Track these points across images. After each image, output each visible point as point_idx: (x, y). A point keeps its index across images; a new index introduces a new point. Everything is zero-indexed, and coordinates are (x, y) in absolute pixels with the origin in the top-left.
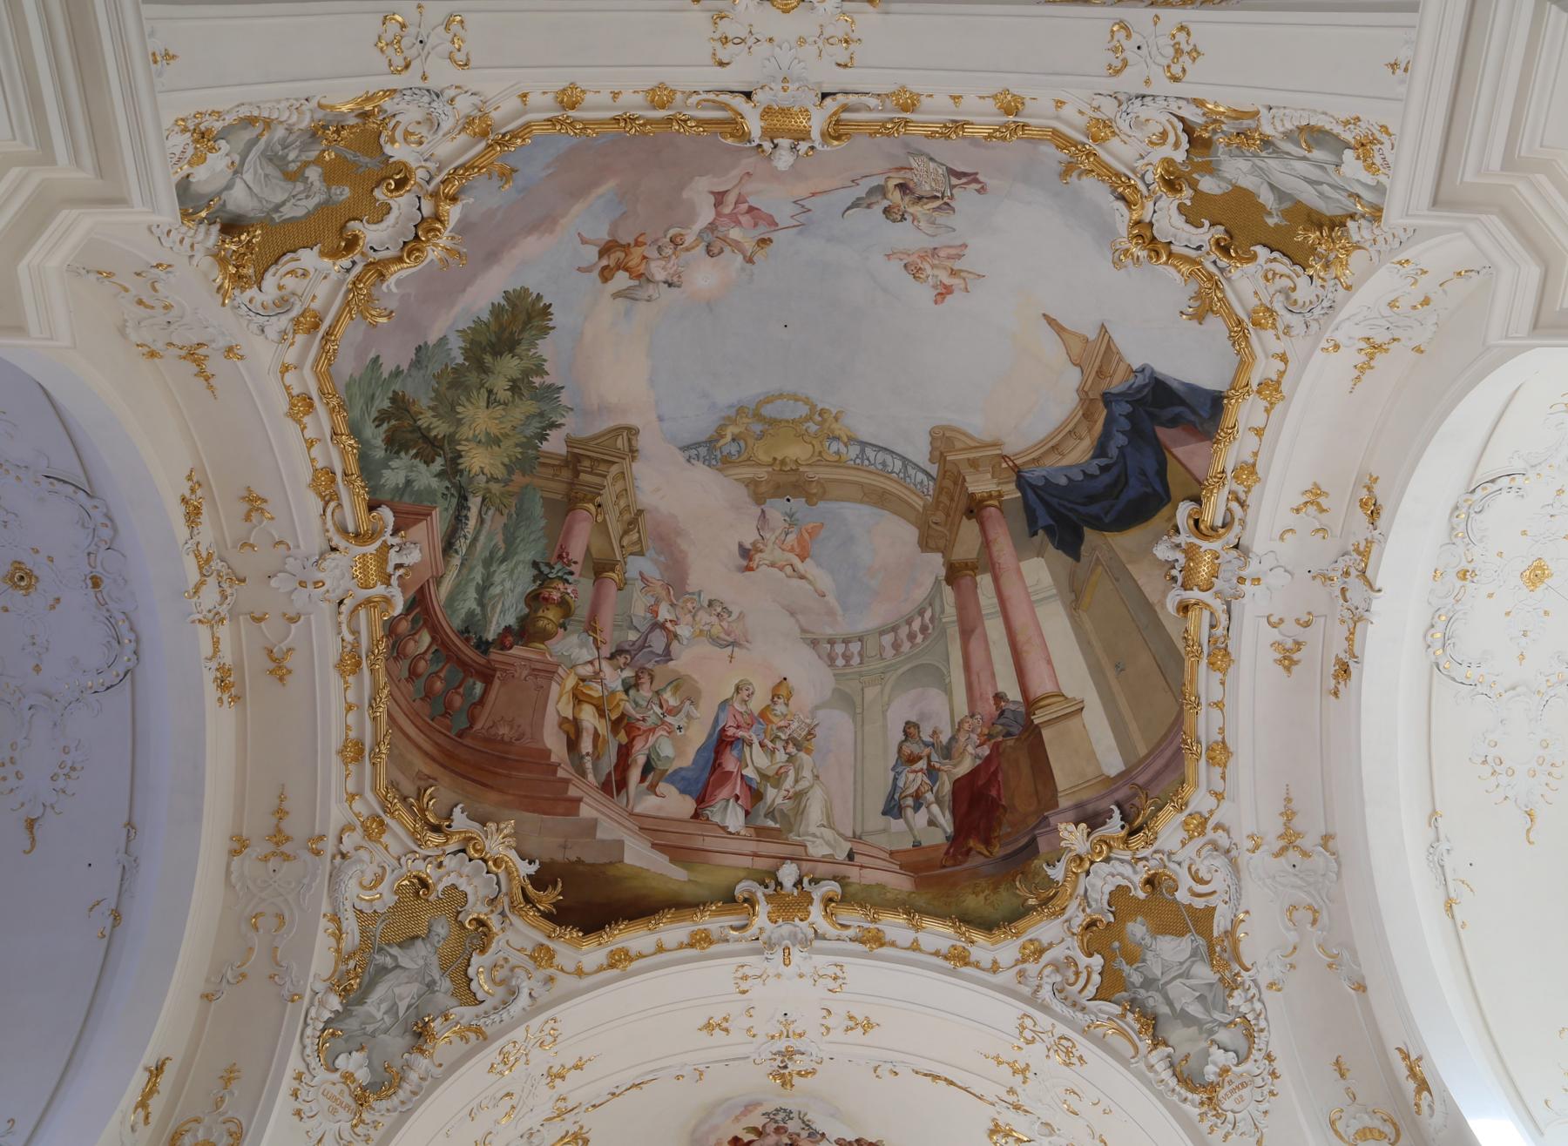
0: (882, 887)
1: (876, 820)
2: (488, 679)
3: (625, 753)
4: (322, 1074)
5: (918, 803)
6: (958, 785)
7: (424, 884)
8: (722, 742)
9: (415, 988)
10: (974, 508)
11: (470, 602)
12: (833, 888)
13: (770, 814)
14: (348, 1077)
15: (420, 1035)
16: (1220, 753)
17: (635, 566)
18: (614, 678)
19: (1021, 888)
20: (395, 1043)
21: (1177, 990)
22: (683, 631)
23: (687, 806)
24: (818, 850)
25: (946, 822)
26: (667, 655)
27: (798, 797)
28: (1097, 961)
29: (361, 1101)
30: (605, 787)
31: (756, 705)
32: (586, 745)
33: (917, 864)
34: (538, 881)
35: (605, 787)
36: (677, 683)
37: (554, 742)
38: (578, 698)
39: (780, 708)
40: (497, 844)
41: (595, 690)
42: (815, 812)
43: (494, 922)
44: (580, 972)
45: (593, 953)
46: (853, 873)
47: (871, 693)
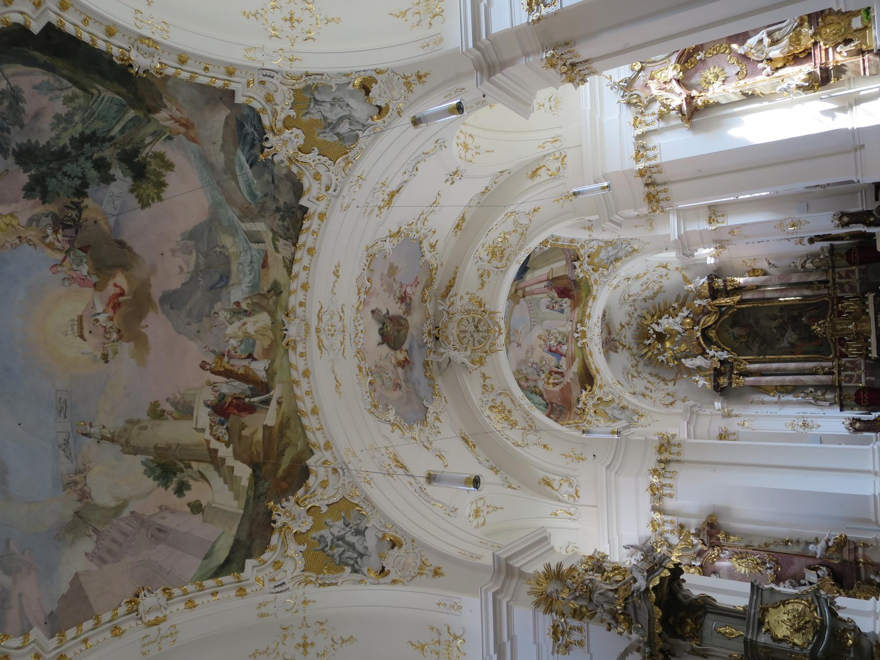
0: (578, 314)
1: (564, 316)
2: (552, 403)
3: (556, 373)
4: (640, 423)
5: (561, 306)
6: (560, 296)
7: (595, 412)
8: (550, 351)
9: (615, 411)
10: (516, 291)
11: (542, 407)
12: (579, 325)
13: (563, 339)
14: (638, 419)
15: (623, 408)
16: (572, 241)
17: (524, 372)
18: (543, 376)
19: (582, 284)
20: (627, 412)
21: (610, 254)
22: (532, 360)
23: (563, 358)
24: (570, 329)
25: (566, 300)
26: (536, 364)
27: (559, 333)
28: (601, 269)
29: (642, 416)
30: (563, 376)
31: (543, 343)
32: (556, 381)
33: (574, 306)
34: (586, 389)
35: (563, 376)
36: (541, 361)
37: (558, 388)
38: (548, 384)
39: (543, 337)
40: (583, 398)
41: (546, 380)
42: (562, 329)
43: (596, 398)
44: (601, 379)
45: (598, 377)
46: (575, 321)
47: (540, 316)
